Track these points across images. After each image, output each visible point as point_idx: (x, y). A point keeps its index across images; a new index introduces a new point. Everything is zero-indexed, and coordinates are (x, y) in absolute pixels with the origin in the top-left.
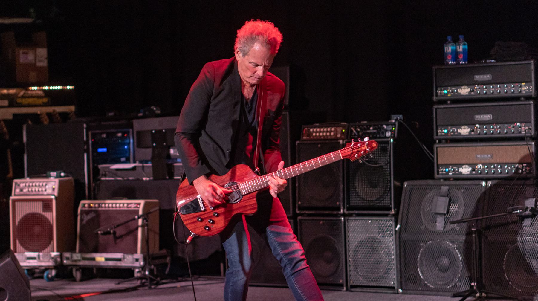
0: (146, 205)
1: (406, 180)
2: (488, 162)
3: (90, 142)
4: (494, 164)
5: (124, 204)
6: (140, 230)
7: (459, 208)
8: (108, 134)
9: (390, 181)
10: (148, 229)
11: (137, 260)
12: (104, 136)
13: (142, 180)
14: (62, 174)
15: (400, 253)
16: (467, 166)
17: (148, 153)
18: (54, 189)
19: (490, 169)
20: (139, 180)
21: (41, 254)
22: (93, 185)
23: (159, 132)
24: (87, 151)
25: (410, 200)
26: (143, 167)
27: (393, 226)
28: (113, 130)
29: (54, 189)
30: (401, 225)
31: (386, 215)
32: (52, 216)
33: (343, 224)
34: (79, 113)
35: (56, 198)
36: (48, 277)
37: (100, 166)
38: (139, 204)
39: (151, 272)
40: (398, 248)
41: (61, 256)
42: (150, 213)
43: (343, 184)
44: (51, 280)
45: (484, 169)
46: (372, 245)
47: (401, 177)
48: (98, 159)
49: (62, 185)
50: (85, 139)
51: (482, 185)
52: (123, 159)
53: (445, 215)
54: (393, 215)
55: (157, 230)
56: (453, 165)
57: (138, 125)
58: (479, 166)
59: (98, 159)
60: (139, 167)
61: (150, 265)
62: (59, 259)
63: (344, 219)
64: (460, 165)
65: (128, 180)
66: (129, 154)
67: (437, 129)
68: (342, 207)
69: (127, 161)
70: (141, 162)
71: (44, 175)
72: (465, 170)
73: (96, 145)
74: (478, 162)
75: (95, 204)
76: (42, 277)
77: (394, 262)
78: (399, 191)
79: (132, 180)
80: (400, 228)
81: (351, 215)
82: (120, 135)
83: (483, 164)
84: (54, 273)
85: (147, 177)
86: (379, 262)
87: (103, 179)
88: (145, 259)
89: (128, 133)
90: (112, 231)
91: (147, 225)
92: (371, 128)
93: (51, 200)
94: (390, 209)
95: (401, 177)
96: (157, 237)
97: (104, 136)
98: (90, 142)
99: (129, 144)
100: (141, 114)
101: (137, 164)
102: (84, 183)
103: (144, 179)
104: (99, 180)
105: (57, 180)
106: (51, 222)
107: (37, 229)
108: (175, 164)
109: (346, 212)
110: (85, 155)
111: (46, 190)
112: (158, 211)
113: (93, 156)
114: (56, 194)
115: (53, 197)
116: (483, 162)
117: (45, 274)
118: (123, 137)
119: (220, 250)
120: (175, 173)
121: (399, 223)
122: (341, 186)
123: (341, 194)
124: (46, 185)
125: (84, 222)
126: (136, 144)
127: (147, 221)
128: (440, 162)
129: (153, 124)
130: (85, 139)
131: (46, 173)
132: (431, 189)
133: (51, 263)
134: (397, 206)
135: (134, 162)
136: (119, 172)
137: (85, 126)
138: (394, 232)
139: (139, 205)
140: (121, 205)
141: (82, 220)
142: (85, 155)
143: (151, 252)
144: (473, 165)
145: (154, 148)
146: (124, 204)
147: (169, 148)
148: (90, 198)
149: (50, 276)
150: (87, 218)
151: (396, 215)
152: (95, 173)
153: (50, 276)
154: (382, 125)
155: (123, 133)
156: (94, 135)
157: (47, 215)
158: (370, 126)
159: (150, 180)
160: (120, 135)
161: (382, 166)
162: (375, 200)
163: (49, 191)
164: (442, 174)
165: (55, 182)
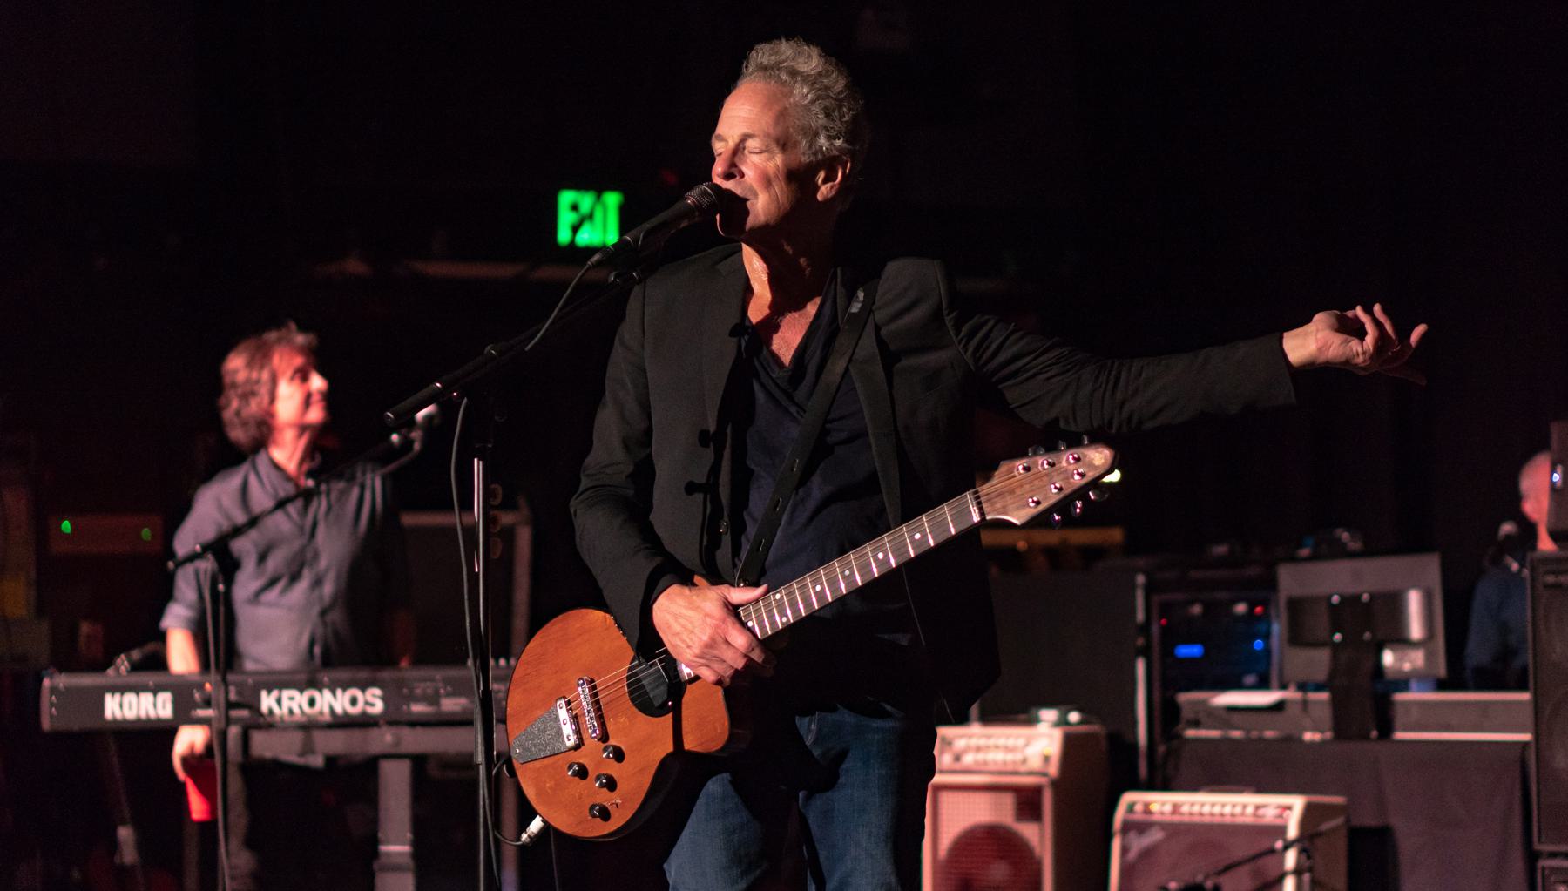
3: (1155, 630)
5: (1245, 806)
8: (1208, 606)
10: (1314, 882)
12: (1197, 609)
13: (1301, 741)
14: (1074, 717)
17: (1318, 661)
18: (1047, 759)
20: (1291, 741)
22: (1161, 749)
23: (1351, 601)
24: (1145, 652)
26: (1305, 704)
28: (1222, 595)
29: (1047, 759)
32: (1038, 837)
34: (1131, 547)
37: (1184, 698)
38: (1289, 808)
42: (1319, 834)
48: (1173, 680)
49: (1071, 744)
50: (1140, 616)
52: (1250, 679)
57: (1293, 580)
59: (1173, 680)
60: (1293, 702)
65: (1261, 740)
66: (1269, 664)
69: (1263, 684)
70: (1302, 687)
71: (1023, 717)
73: (1172, 637)
75: (1163, 804)
82: (1241, 608)
85: (1315, 729)
87: (1191, 733)
89: (1265, 603)
91: (1310, 870)
97: (1197, 609)
98: (1155, 630)
99: (1267, 637)
100: (1305, 552)
101: (1291, 694)
103: (1308, 736)
104: (1179, 737)
105: (1057, 734)
106: (1037, 850)
108: (1400, 697)
110: (1141, 667)
112: (1343, 832)
114: (1053, 770)
120: (1399, 719)
124: (1027, 745)
125: (1132, 855)
127: (1309, 857)
135: (1283, 687)
136: (1236, 717)
137: (1141, 579)
141: (1125, 850)
142: (1141, 667)
145: (1336, 647)
146: (1245, 806)
148: (1151, 786)
150: (1139, 843)
152: (1167, 716)
155: (1252, 606)
159: (1324, 743)
160: (1241, 608)
165: (1050, 736)
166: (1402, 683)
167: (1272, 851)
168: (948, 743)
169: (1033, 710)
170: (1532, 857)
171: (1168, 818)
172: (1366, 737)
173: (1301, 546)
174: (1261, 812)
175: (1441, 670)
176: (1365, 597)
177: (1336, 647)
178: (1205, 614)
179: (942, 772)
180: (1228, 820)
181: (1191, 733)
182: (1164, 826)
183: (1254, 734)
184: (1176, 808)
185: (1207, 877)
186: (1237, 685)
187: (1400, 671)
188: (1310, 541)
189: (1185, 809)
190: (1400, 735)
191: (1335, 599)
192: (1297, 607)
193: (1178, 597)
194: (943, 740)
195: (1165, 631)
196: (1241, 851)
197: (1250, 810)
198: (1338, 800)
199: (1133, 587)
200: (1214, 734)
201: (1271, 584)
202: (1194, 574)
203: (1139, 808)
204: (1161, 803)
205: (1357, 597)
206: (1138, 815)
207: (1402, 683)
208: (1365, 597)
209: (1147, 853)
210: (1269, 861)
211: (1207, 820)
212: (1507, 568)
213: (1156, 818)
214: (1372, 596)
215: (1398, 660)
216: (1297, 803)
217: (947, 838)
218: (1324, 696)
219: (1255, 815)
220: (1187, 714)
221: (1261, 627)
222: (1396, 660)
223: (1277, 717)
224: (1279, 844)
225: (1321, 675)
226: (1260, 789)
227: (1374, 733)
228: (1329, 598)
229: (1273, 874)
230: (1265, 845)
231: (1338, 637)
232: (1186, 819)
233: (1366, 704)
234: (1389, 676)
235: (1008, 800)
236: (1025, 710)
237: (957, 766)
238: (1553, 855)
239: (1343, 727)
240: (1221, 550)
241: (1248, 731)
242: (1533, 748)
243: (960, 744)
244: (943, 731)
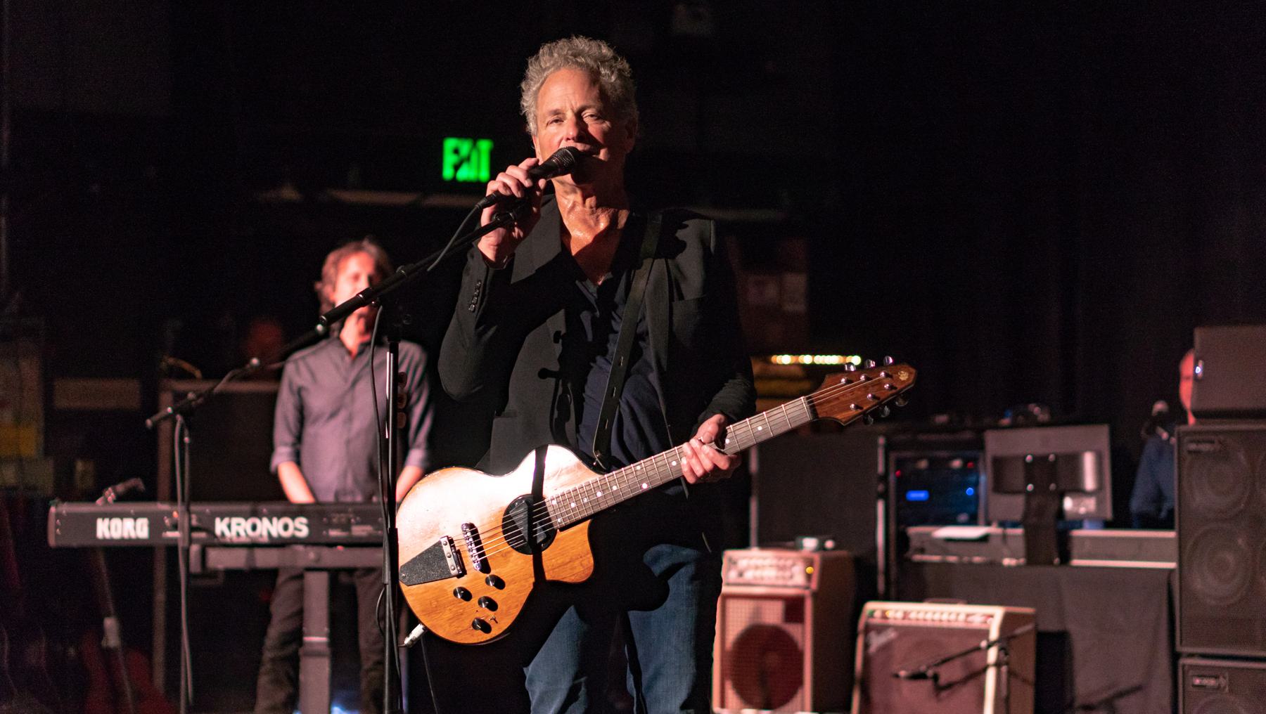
0: (1008, 618)
3: (892, 478)
6: (991, 676)
8: (932, 462)
10: (1010, 673)
12: (923, 464)
13: (1000, 565)
14: (829, 544)
17: (1015, 505)
18: (809, 577)
20: (994, 565)
22: (894, 570)
23: (1040, 460)
24: (884, 496)
26: (1004, 537)
28: (943, 454)
32: (804, 635)
35: (815, 595)
37: (913, 531)
38: (991, 616)
42: (1014, 637)
48: (905, 515)
50: (881, 468)
55: (1030, 674)
57: (997, 443)
59: (905, 515)
65: (971, 564)
69: (973, 521)
70: (1003, 524)
71: (790, 544)
73: (905, 485)
75: (896, 611)
79: (979, 565)
82: (957, 464)
85: (1012, 556)
89: (975, 460)
90: (930, 673)
91: (1007, 664)
96: (1030, 692)
97: (923, 464)
98: (892, 478)
99: (976, 485)
100: (1006, 421)
101: (993, 530)
102: (875, 566)
103: (1007, 562)
104: (909, 560)
106: (800, 645)
107: (773, 659)
108: (1077, 533)
110: (880, 507)
111: (791, 577)
113: (898, 509)
114: (814, 585)
115: (807, 593)
118: (964, 471)
120: (1075, 552)
126: (991, 486)
127: (1006, 654)
129: (1029, 443)
130: (881, 468)
135: (988, 524)
136: (951, 546)
137: (881, 441)
139: (989, 618)
142: (880, 507)
145: (1029, 495)
146: (958, 615)
147: (1061, 496)
148: (887, 598)
150: (877, 641)
152: (900, 542)
156: (900, 463)
157: (794, 630)
159: (1018, 567)
160: (957, 464)
166: (1078, 523)
167: (978, 649)
168: (733, 562)
169: (798, 539)
170: (1175, 657)
171: (900, 623)
172: (1051, 563)
173: (1003, 416)
174: (970, 619)
175: (1109, 514)
176: (1052, 457)
177: (1029, 495)
178: (930, 467)
179: (728, 584)
180: (945, 625)
181: (918, 558)
182: (896, 628)
183: (966, 559)
184: (906, 615)
185: (929, 667)
186: (952, 521)
187: (1077, 514)
188: (1010, 413)
189: (913, 616)
190: (1076, 562)
191: (1029, 458)
192: (999, 464)
193: (908, 454)
195: (900, 480)
196: (955, 649)
197: (962, 617)
198: (1028, 610)
199: (875, 445)
200: (936, 558)
201: (980, 445)
202: (922, 437)
203: (878, 614)
204: (895, 611)
205: (1045, 458)
206: (877, 620)
207: (1078, 523)
208: (1052, 457)
209: (886, 647)
210: (975, 655)
211: (929, 624)
212: (1160, 437)
213: (891, 622)
214: (1057, 457)
215: (1076, 505)
216: (998, 612)
218: (1019, 531)
219: (966, 621)
220: (915, 543)
221: (972, 479)
222: (1074, 505)
223: (983, 547)
224: (984, 644)
225: (1018, 516)
226: (970, 602)
227: (1057, 561)
228: (1025, 457)
229: (979, 665)
230: (971, 644)
231: (1030, 487)
232: (914, 623)
233: (1051, 539)
234: (1068, 517)
236: (793, 540)
237: (741, 580)
238: (1191, 655)
239: (1033, 555)
240: (942, 419)
241: (961, 557)
242: (1177, 576)
243: (743, 563)
244: (730, 554)
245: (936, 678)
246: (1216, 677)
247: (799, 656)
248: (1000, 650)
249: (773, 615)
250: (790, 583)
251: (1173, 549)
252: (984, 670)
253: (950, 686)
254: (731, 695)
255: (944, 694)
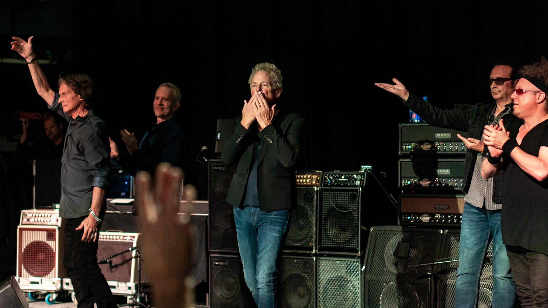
1: (372, 226)
2: (445, 212)
4: (450, 215)
5: (120, 236)
6: (133, 261)
7: (418, 253)
9: (358, 226)
10: (140, 260)
11: (130, 288)
15: (364, 291)
16: (426, 215)
19: (447, 219)
21: (43, 279)
25: (375, 243)
27: (359, 267)
30: (366, 267)
31: (354, 257)
32: (55, 245)
33: (314, 263)
36: (49, 300)
38: (134, 237)
39: (142, 299)
40: (363, 287)
41: (62, 282)
43: (316, 227)
44: (52, 303)
45: (441, 219)
46: (340, 283)
47: (368, 222)
51: (439, 233)
53: (406, 258)
54: (360, 257)
56: (415, 214)
58: (438, 216)
61: (141, 293)
62: (59, 285)
63: (316, 259)
64: (421, 214)
67: (401, 180)
68: (314, 248)
72: (425, 219)
74: (437, 211)
76: (43, 300)
77: (359, 300)
78: (365, 235)
80: (365, 269)
81: (322, 255)
83: (441, 215)
84: (55, 296)
86: (346, 299)
88: (137, 287)
91: (140, 257)
92: (343, 177)
93: (54, 230)
94: (357, 252)
95: (368, 222)
107: (41, 256)
109: (318, 253)
114: (59, 224)
116: (441, 211)
117: (47, 298)
119: (206, 281)
121: (365, 264)
122: (315, 229)
123: (314, 236)
128: (403, 210)
131: (52, 205)
132: (395, 235)
133: (54, 288)
134: (363, 248)
138: (360, 272)
140: (118, 237)
143: (142, 282)
144: (432, 215)
146: (120, 236)
149: (51, 300)
151: (362, 258)
153: (51, 300)
154: (352, 175)
158: (342, 175)
161: (351, 212)
162: (344, 243)
163: (54, 222)
164: (405, 221)
167: (129, 251)
170: (208, 253)
179: (22, 224)
185: (108, 259)
194: (24, 214)
197: (122, 237)
210: (128, 253)
217: (24, 247)
224: (130, 249)
229: (128, 258)
230: (126, 249)
235: (45, 234)
237: (28, 223)
238: (214, 253)
242: (209, 219)
243: (29, 215)
245: (111, 263)
246: (224, 262)
247: (55, 254)
248: (137, 251)
249: (42, 237)
250: (49, 224)
251: (208, 209)
252: (131, 259)
253: (116, 266)
254: (23, 270)
255: (114, 269)
